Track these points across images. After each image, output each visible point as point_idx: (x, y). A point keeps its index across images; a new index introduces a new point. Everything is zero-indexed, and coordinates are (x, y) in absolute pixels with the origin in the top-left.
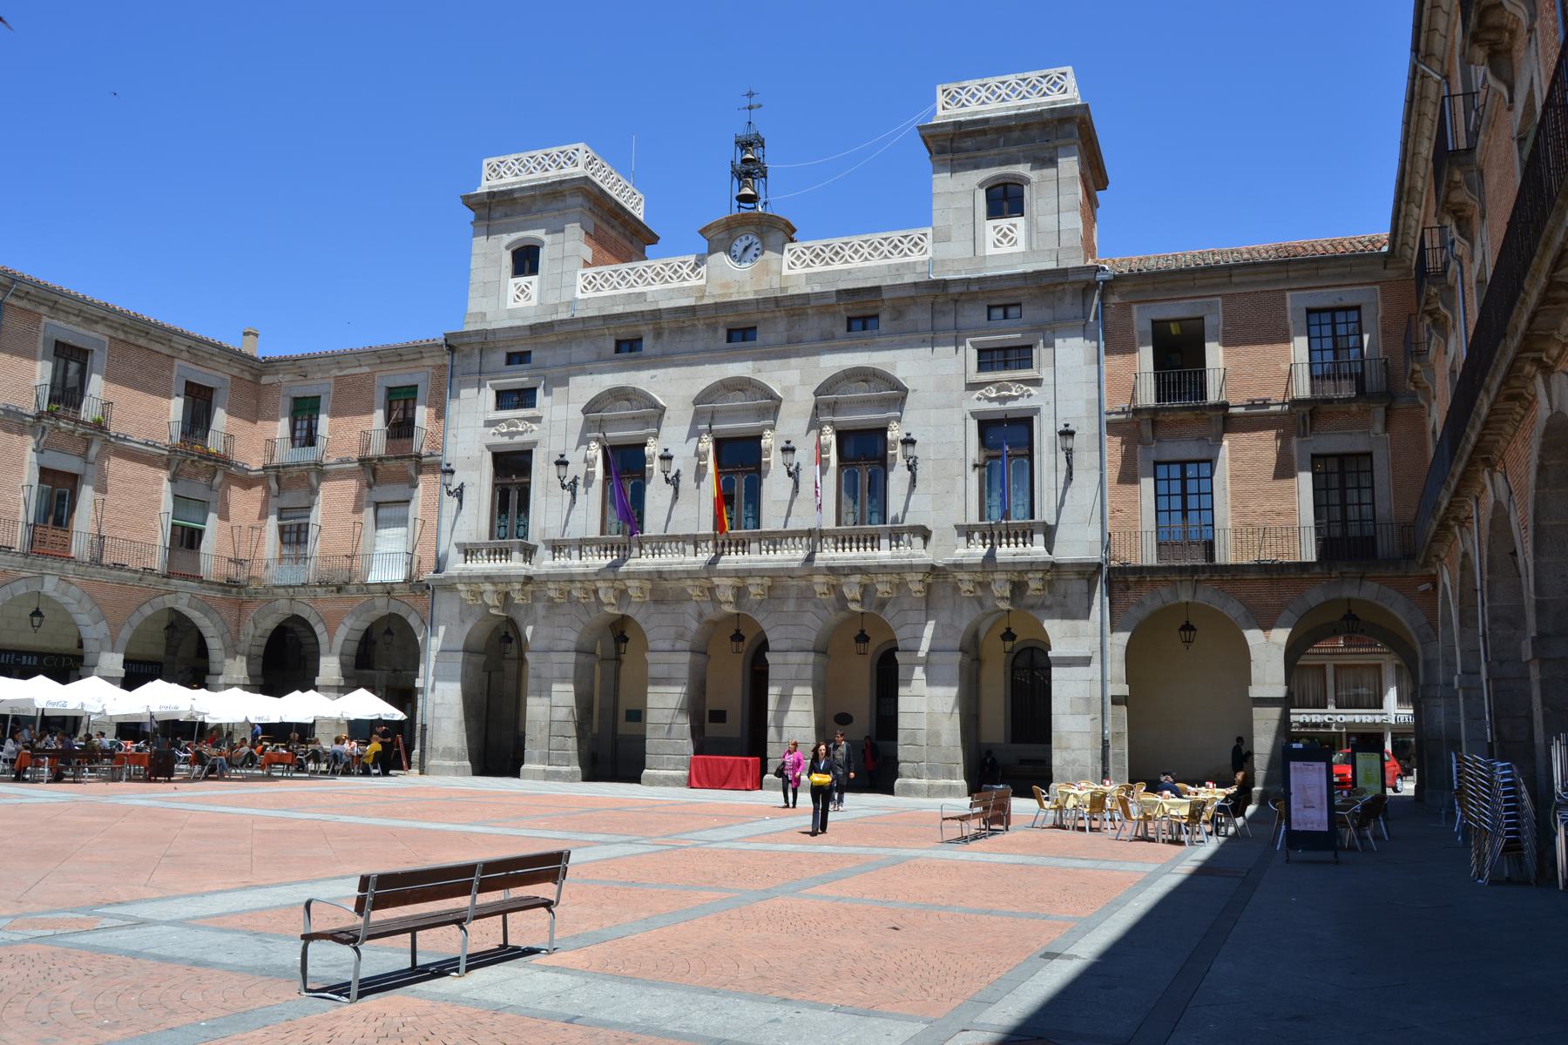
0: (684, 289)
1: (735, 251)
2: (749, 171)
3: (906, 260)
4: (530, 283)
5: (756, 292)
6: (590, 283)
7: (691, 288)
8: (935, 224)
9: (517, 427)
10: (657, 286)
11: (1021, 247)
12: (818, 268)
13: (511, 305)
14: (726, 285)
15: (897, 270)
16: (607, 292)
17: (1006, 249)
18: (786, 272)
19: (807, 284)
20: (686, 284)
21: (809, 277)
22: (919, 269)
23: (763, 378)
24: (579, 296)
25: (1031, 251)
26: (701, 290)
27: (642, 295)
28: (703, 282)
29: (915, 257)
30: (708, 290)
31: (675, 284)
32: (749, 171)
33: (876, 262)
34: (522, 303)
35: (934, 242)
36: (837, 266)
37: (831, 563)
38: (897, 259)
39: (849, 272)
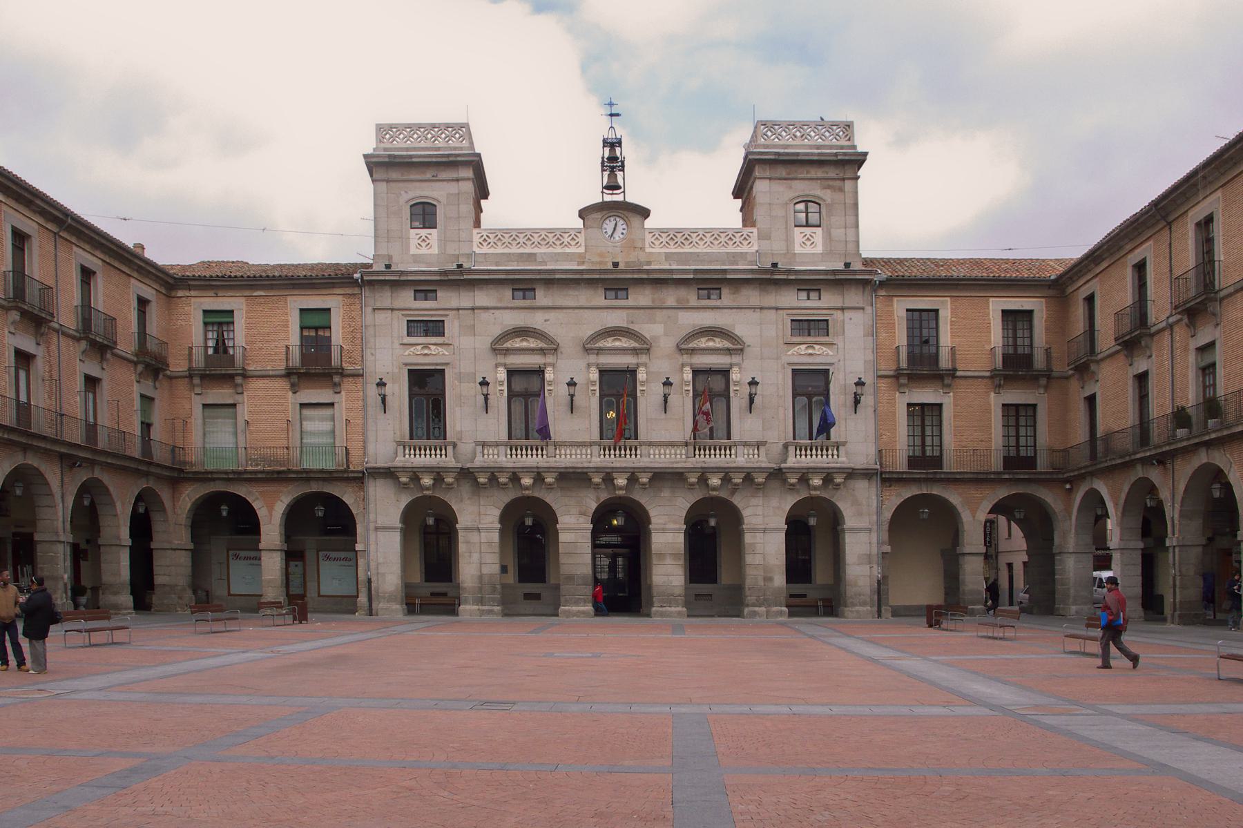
0: (568, 254)
1: (606, 229)
2: (613, 164)
3: (739, 250)
4: (430, 234)
5: (627, 263)
6: (485, 240)
7: (573, 254)
8: (758, 225)
9: (427, 353)
10: (543, 250)
11: (819, 249)
12: (673, 249)
13: (413, 251)
14: (601, 255)
15: (734, 257)
16: (500, 250)
17: (808, 249)
18: (648, 250)
19: (666, 260)
20: (567, 250)
21: (668, 256)
22: (749, 258)
23: (636, 327)
24: (477, 251)
25: (828, 254)
26: (581, 258)
27: (531, 257)
28: (582, 250)
29: (744, 249)
30: (587, 257)
31: (558, 250)
32: (613, 164)
33: (715, 249)
34: (424, 251)
35: (759, 239)
36: (687, 249)
37: (704, 465)
38: (731, 249)
39: (698, 254)
